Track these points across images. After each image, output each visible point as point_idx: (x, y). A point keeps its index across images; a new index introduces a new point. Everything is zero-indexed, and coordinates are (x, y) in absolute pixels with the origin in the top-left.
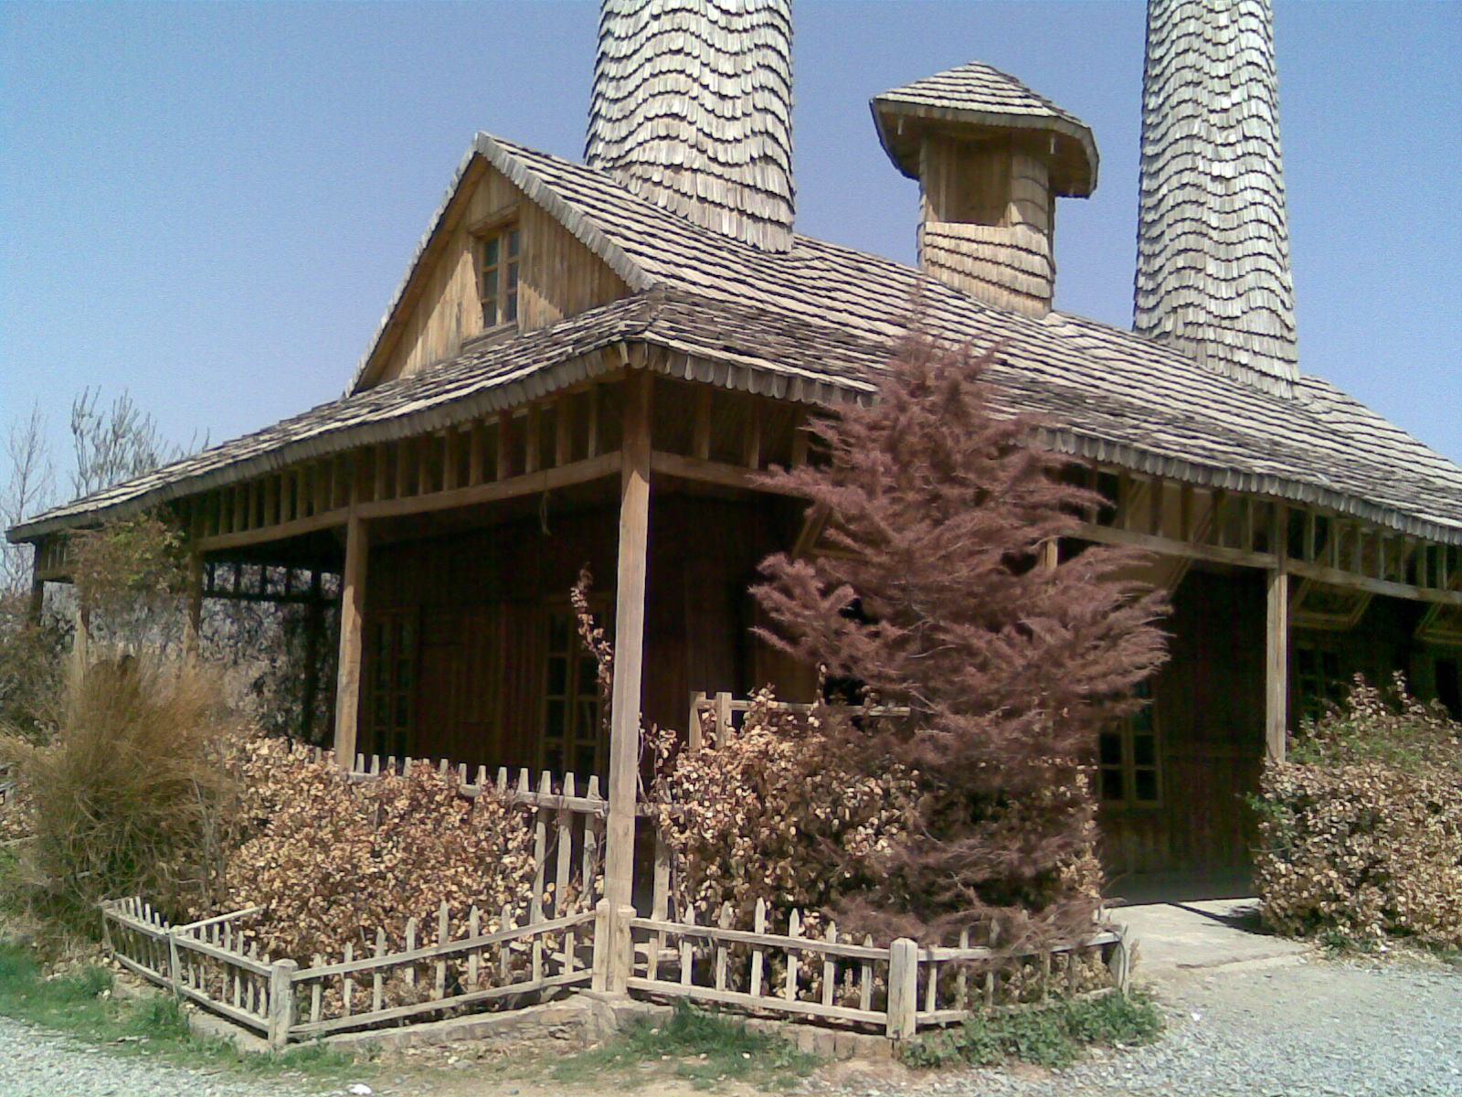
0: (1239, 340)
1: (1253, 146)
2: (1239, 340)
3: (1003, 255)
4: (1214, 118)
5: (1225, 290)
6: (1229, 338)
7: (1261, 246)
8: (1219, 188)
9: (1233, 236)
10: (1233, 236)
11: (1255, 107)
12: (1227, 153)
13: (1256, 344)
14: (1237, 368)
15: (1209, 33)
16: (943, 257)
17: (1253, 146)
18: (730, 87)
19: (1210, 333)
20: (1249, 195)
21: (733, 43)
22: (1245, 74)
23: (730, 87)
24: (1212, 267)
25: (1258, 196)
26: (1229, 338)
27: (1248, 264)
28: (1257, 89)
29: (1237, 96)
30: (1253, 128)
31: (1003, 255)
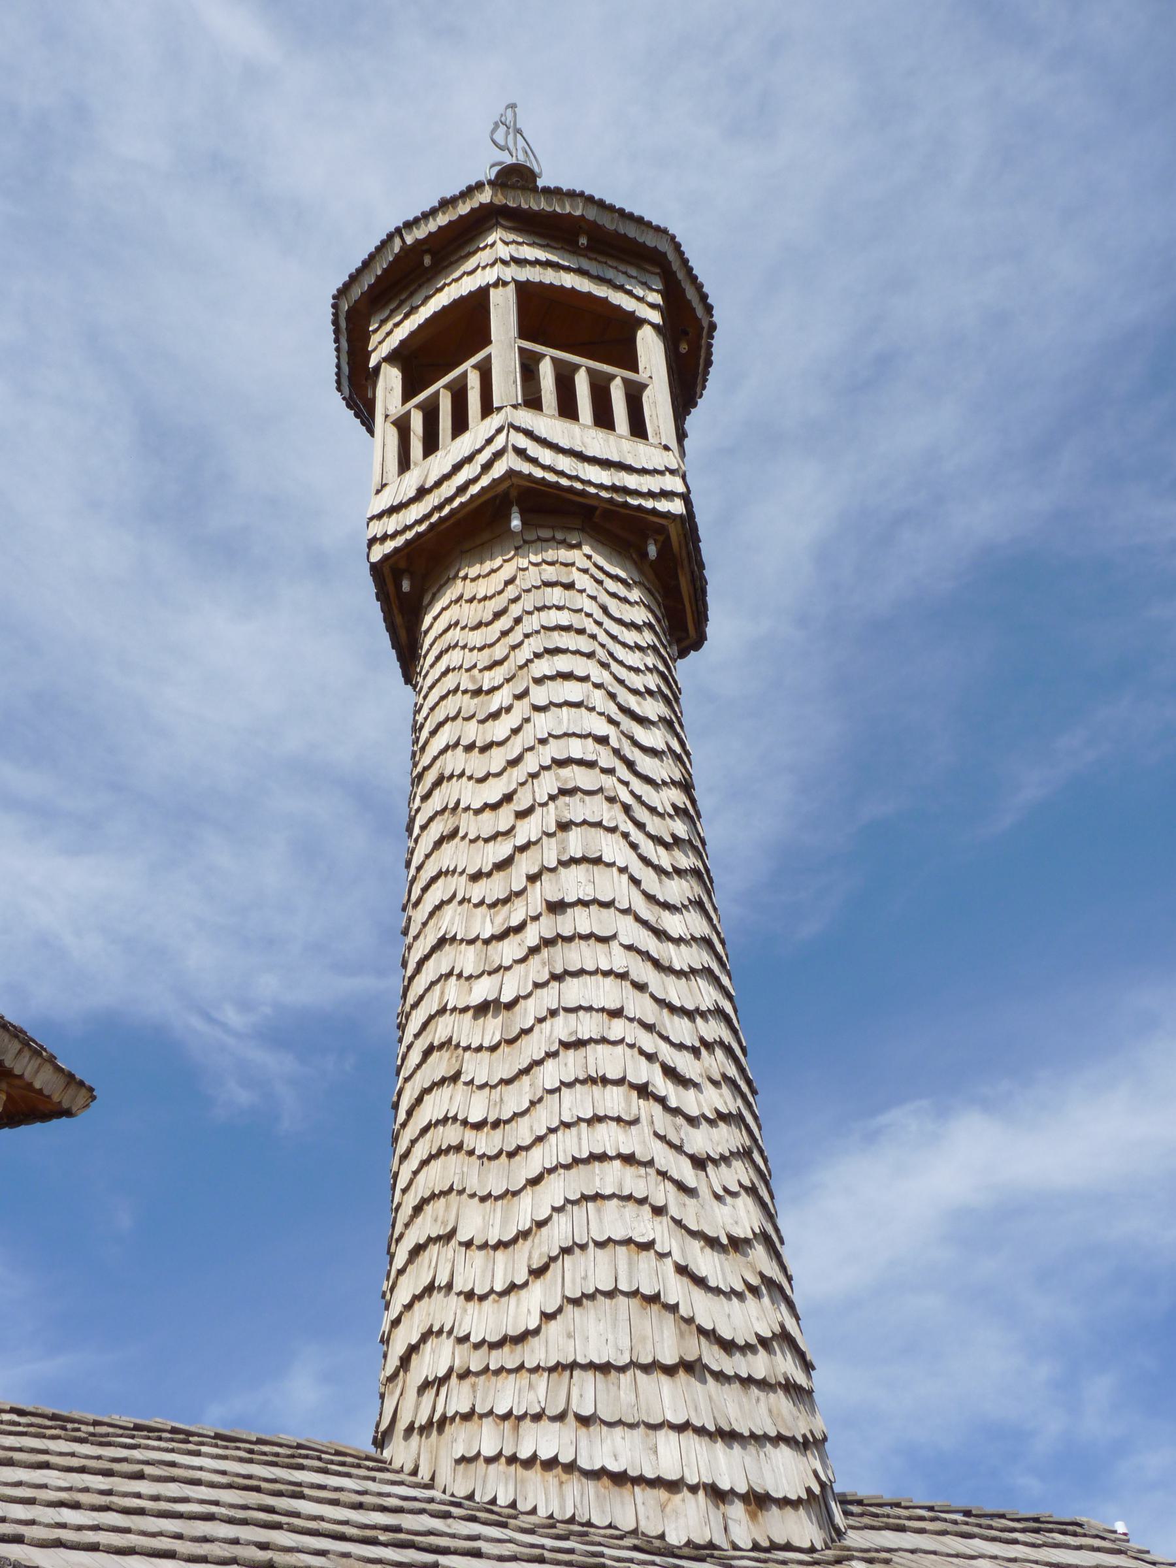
1: (581, 921)
4: (477, 891)
5: (509, 1267)
6: (507, 1395)
7: (608, 1138)
8: (492, 1029)
9: (522, 1133)
10: (522, 1133)
12: (510, 950)
13: (586, 1394)
14: (535, 1475)
15: (471, 732)
17: (581, 921)
19: (458, 1398)
20: (562, 1028)
22: (548, 784)
24: (475, 1222)
25: (588, 1026)
26: (507, 1395)
27: (556, 1190)
29: (528, 830)
30: (573, 883)
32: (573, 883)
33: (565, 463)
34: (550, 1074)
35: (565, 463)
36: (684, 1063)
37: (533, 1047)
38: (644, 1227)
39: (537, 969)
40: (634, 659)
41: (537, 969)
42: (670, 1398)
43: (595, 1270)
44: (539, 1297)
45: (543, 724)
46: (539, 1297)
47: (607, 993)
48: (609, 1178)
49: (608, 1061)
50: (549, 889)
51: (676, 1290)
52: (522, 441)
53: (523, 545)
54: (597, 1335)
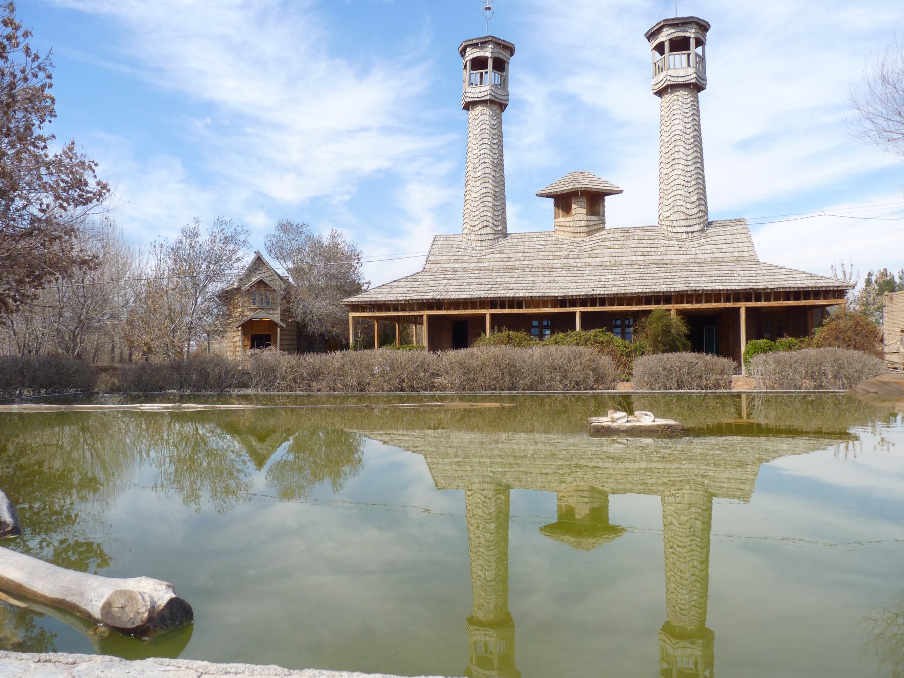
0: (669, 223)
2: (669, 223)
3: (571, 224)
7: (679, 192)
9: (669, 192)
10: (669, 192)
11: (676, 149)
16: (558, 228)
17: (676, 161)
18: (476, 214)
20: (673, 178)
21: (476, 204)
23: (476, 214)
25: (676, 177)
28: (678, 143)
30: (676, 155)
31: (571, 224)
32: (676, 155)
33: (676, 79)
34: (672, 184)
35: (676, 79)
36: (689, 179)
37: (670, 180)
38: (681, 203)
39: (671, 169)
40: (687, 111)
41: (671, 169)
42: (683, 223)
43: (676, 209)
44: (670, 213)
45: (673, 129)
46: (670, 213)
47: (679, 172)
48: (678, 197)
49: (678, 182)
50: (673, 157)
51: (685, 210)
52: (669, 78)
53: (671, 93)
54: (676, 217)
